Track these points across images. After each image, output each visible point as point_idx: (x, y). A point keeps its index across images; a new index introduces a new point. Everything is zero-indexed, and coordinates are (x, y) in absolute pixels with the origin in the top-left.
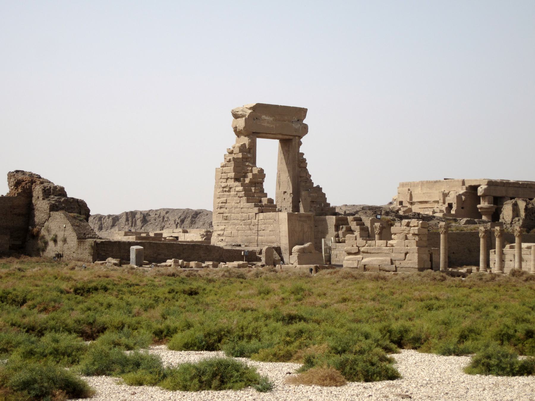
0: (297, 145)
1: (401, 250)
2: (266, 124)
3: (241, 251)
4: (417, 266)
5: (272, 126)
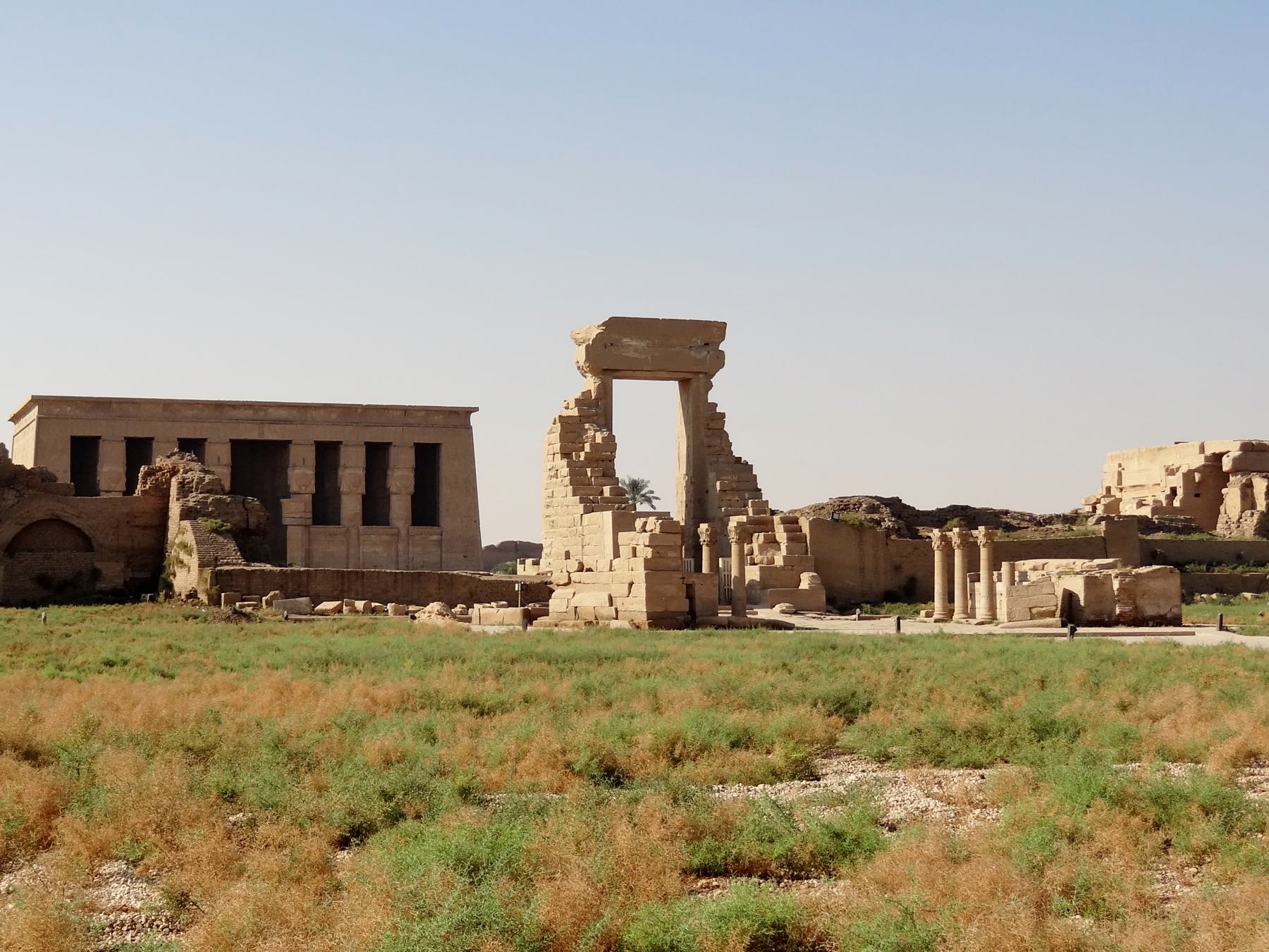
0: (702, 391)
1: (624, 578)
2: (631, 354)
3: (514, 583)
4: (645, 610)
5: (645, 357)
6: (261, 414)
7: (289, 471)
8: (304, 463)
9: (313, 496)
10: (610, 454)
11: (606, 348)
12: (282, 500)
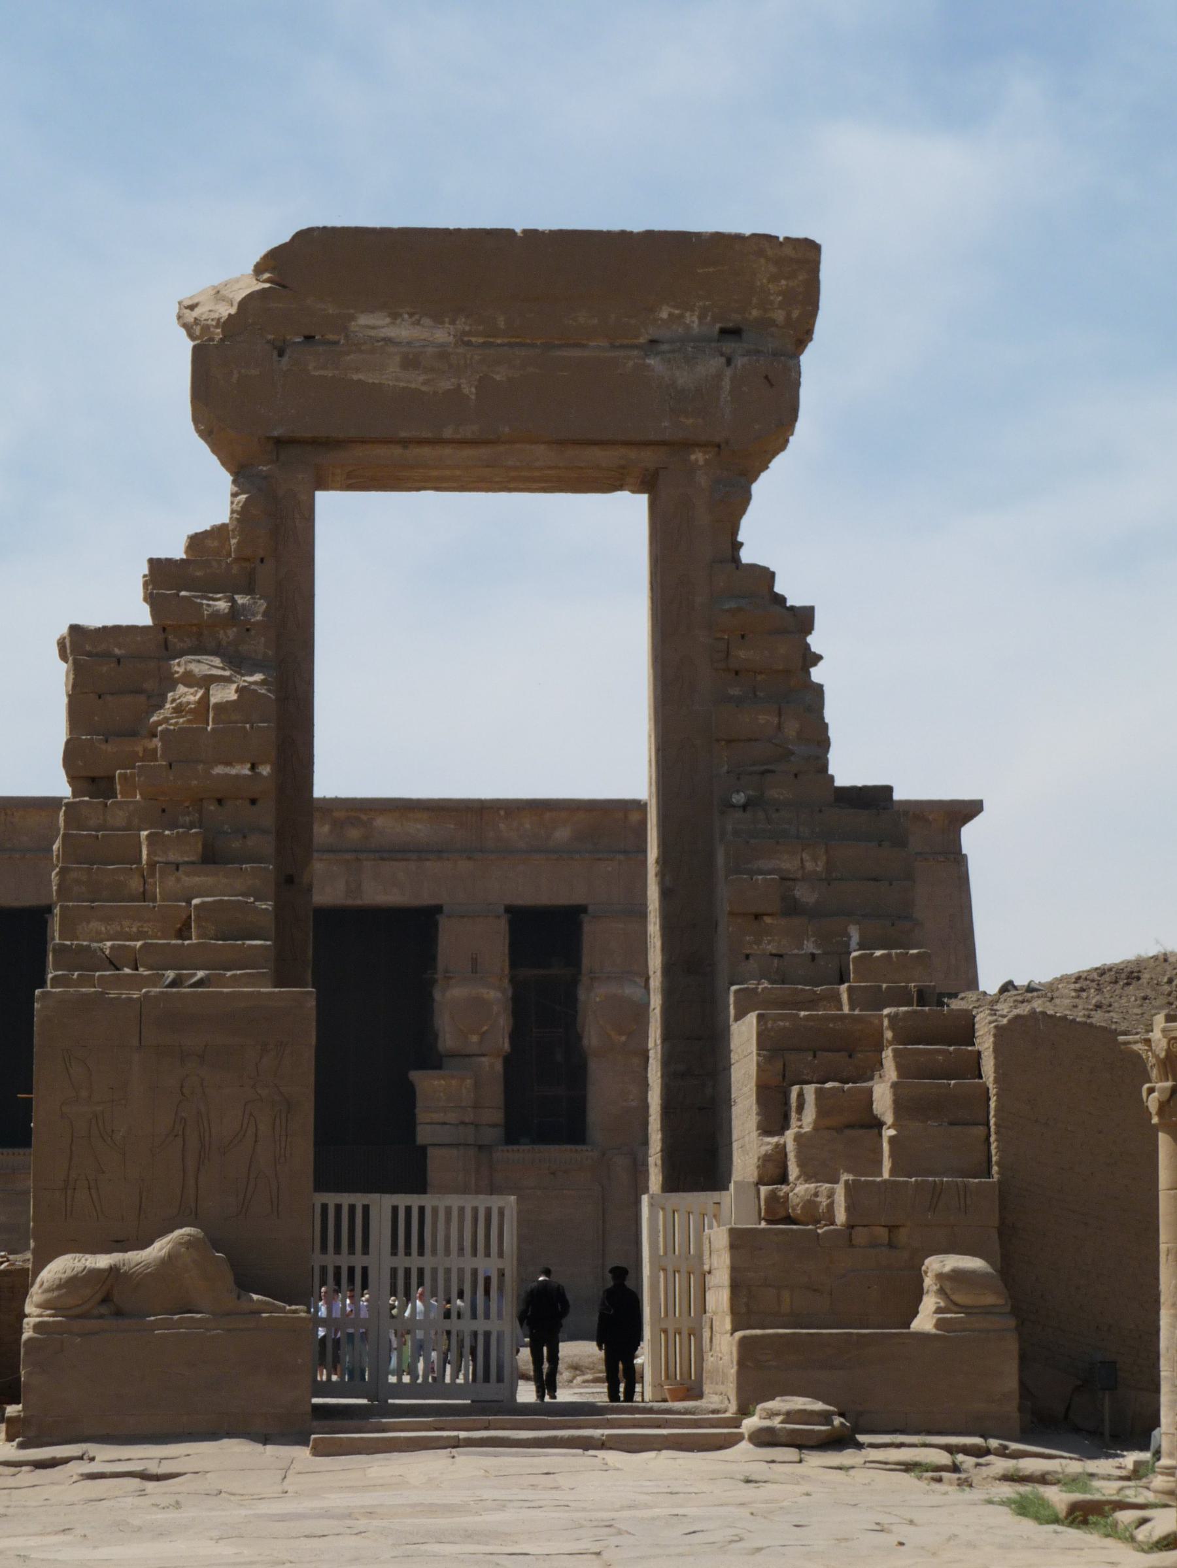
5: (446, 384)
6: (354, 834)
8: (474, 971)
9: (508, 1060)
10: (246, 770)
12: (415, 1076)
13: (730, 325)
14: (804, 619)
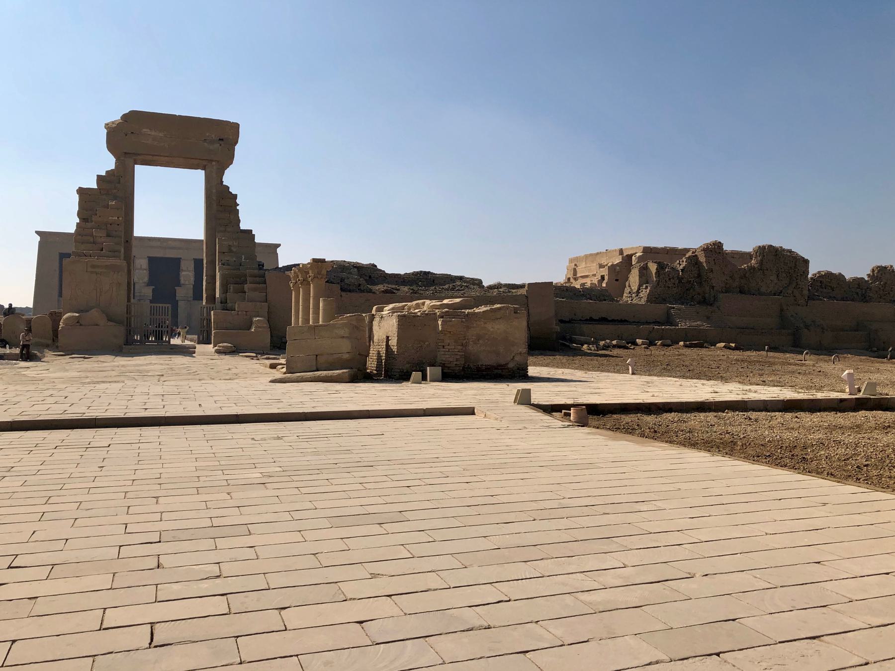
7: (180, 273)
11: (126, 135)
13: (221, 138)
14: (235, 196)
